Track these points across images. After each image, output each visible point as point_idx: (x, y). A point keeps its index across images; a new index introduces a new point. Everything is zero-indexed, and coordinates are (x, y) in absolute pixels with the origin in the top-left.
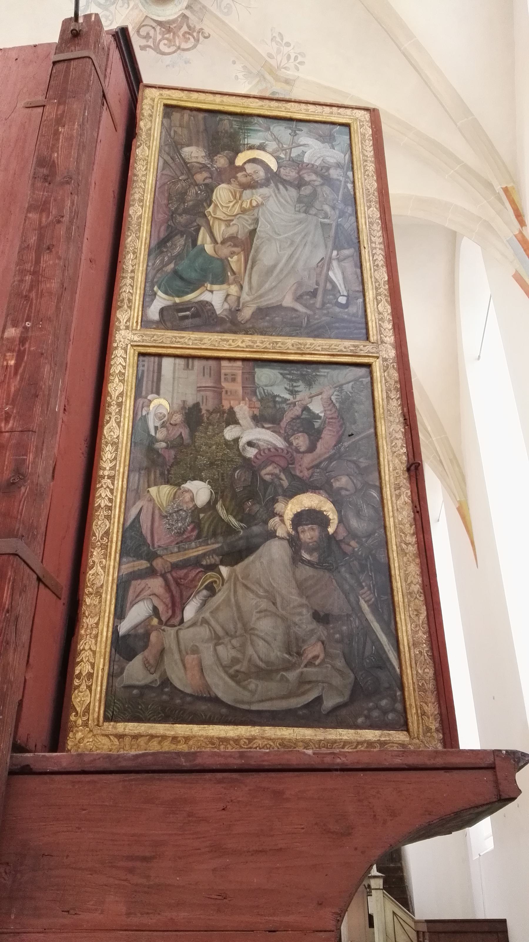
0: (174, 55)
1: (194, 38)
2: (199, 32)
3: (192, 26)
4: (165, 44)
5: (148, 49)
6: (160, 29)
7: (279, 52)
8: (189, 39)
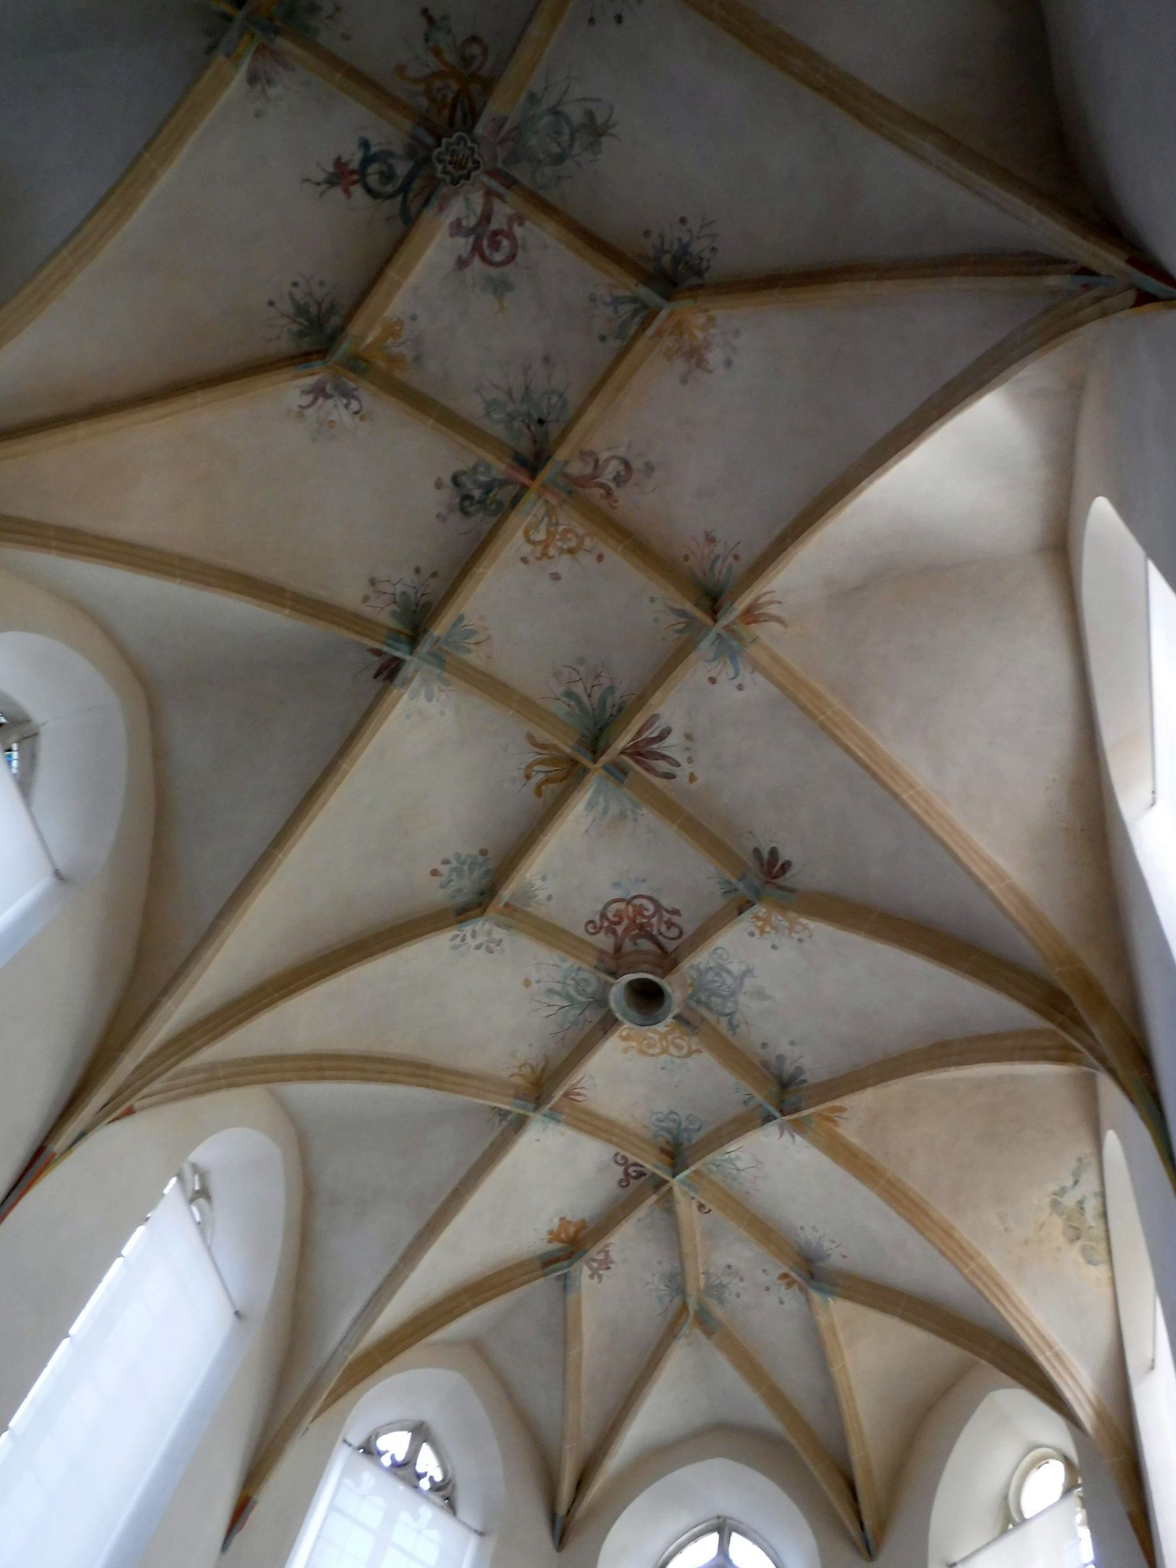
0: (634, 894)
1: (608, 919)
2: (601, 928)
3: (610, 935)
4: (647, 910)
5: (670, 909)
6: (653, 930)
7: (489, 933)
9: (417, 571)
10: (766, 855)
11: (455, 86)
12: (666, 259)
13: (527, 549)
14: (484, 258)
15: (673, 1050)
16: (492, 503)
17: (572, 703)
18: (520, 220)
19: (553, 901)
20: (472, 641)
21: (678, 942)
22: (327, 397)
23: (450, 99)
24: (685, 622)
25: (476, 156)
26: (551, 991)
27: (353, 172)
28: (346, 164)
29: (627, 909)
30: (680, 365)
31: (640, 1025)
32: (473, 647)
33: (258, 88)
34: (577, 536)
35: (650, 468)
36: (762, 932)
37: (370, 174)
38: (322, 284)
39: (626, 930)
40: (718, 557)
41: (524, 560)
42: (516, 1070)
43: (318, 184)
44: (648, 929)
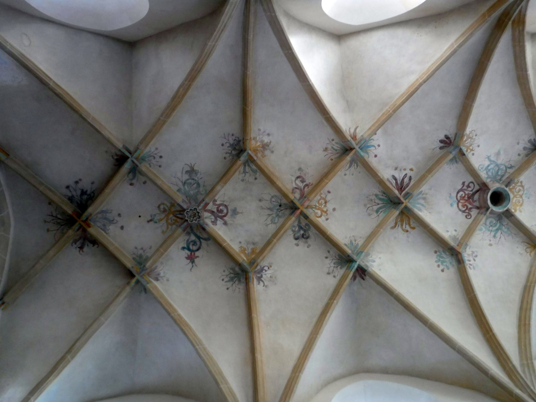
0: (455, 199)
1: (465, 210)
2: (469, 213)
3: (472, 210)
4: (462, 195)
5: (462, 185)
6: (470, 194)
7: (468, 255)
8: (464, 208)
9: (327, 258)
10: (442, 145)
11: (171, 216)
12: (234, 152)
13: (323, 218)
14: (225, 216)
15: (521, 193)
16: (306, 227)
17: (380, 211)
18: (215, 201)
19: (457, 230)
20: (354, 242)
21: (475, 184)
22: (262, 276)
23: (175, 218)
24: (354, 164)
25: (193, 209)
26: (494, 236)
27: (191, 254)
28: (188, 256)
29: (462, 202)
30: (267, 152)
31: (509, 202)
32: (357, 242)
33: (159, 278)
34: (320, 199)
35: (300, 169)
36: (472, 150)
37: (193, 249)
38: (224, 271)
39: (470, 204)
40: (332, 148)
41: (327, 219)
42: (528, 254)
43: (193, 266)
44: (470, 195)
